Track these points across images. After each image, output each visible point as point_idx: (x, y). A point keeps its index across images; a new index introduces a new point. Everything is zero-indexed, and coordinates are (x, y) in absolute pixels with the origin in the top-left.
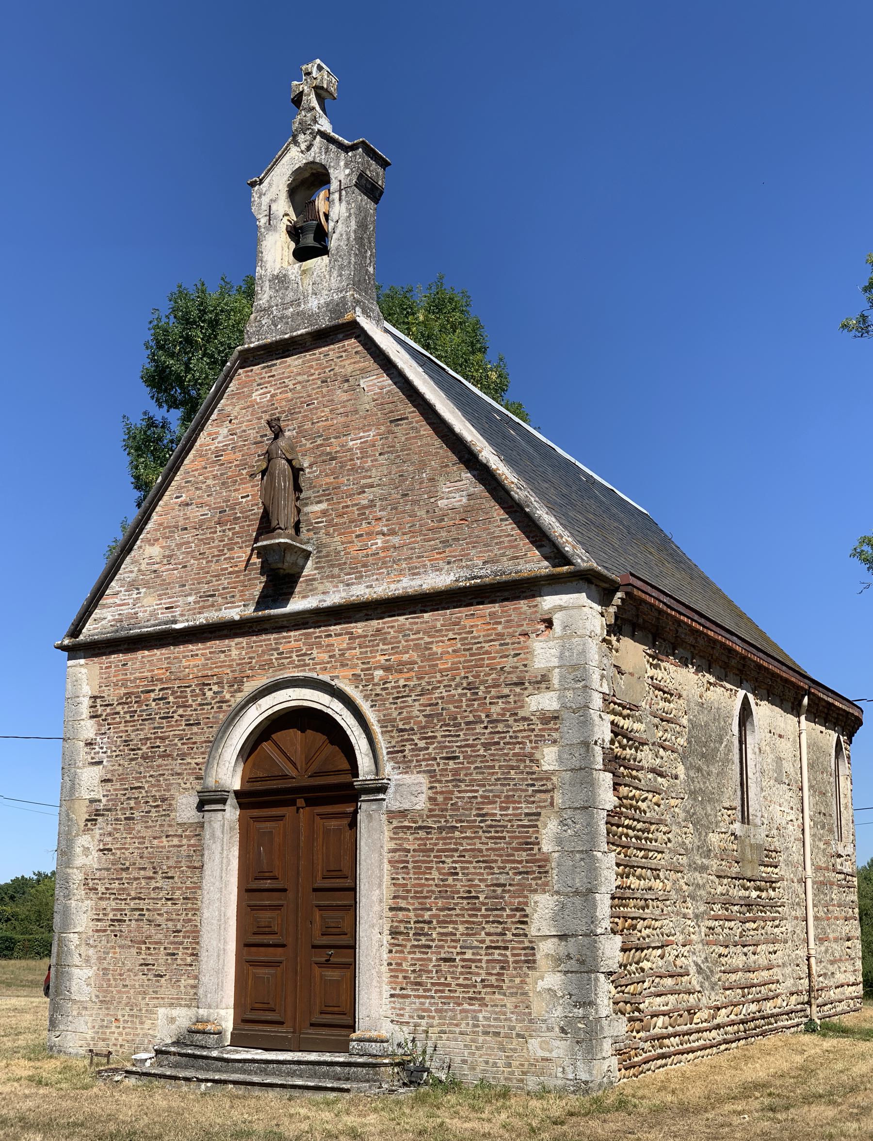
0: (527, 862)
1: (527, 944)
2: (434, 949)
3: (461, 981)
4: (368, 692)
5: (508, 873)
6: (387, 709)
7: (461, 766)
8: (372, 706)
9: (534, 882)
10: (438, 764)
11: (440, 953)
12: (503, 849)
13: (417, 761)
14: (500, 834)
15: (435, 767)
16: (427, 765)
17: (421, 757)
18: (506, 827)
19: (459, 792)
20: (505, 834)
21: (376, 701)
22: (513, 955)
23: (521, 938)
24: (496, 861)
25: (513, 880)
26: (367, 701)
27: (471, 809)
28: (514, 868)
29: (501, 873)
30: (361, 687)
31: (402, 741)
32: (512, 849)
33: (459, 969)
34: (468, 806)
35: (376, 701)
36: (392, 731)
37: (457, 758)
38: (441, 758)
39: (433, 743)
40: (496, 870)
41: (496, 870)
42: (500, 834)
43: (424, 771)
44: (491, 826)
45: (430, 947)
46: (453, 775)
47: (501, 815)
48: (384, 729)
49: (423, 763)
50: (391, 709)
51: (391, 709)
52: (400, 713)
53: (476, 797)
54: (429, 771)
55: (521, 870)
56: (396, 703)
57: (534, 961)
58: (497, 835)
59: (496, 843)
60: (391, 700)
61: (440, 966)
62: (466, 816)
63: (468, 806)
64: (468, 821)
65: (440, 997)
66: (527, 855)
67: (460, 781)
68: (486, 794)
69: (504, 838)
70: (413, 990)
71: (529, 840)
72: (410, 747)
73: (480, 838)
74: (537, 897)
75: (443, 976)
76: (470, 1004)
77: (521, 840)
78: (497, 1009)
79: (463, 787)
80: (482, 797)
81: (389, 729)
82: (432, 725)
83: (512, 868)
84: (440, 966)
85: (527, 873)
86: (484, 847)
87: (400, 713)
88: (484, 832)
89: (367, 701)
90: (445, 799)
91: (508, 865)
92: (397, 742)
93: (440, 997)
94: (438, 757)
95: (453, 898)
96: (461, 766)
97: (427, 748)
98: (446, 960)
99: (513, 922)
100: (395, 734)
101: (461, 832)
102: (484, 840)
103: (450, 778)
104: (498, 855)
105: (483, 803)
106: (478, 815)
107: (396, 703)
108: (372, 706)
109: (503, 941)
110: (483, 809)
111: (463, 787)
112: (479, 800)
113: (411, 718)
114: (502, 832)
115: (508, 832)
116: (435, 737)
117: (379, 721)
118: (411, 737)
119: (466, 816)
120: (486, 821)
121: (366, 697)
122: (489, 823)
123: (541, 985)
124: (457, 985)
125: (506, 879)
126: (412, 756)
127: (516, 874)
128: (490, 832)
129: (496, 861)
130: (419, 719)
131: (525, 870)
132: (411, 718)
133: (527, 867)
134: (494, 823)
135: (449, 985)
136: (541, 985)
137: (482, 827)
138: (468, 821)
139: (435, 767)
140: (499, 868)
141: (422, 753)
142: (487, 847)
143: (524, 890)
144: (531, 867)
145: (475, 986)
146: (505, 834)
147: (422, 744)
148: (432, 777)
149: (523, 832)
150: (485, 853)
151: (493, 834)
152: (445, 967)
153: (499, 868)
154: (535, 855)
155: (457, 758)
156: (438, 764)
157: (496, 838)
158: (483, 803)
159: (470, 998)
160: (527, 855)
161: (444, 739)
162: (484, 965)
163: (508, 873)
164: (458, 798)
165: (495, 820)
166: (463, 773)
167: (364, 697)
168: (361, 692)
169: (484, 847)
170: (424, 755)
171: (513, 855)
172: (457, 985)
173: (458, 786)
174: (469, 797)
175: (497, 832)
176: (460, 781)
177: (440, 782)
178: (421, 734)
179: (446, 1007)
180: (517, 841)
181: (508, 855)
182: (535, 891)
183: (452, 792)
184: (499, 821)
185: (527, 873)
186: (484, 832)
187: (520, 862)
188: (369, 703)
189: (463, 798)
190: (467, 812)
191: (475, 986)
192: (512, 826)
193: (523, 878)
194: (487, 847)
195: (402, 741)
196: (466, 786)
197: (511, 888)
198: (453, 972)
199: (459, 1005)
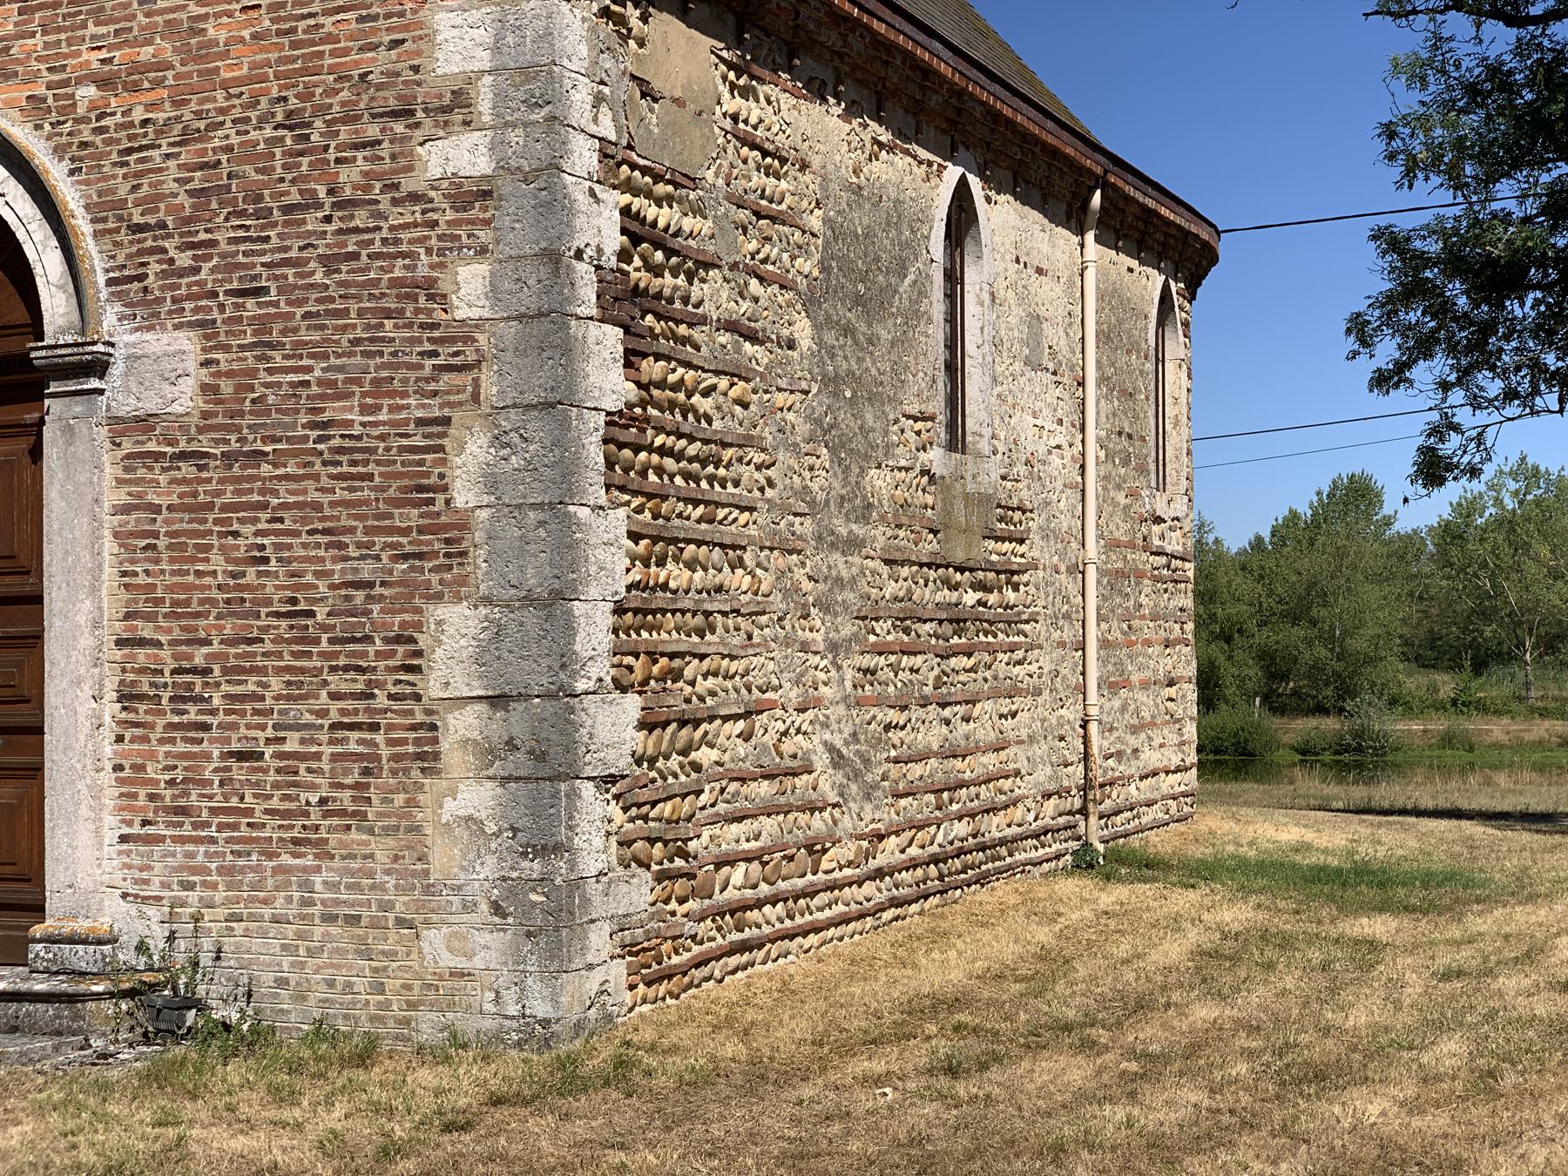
0: (420, 531)
1: (420, 718)
2: (215, 733)
3: (275, 803)
4: (64, 139)
5: (378, 558)
6: (106, 178)
7: (273, 310)
8: (72, 172)
9: (435, 578)
10: (222, 307)
11: (228, 741)
12: (367, 502)
13: (174, 300)
14: (361, 469)
15: (215, 314)
16: (196, 310)
17: (183, 291)
18: (372, 451)
19: (270, 371)
20: (371, 467)
21: (81, 159)
22: (391, 743)
23: (408, 705)
24: (351, 530)
25: (391, 572)
26: (61, 159)
27: (297, 411)
28: (392, 546)
29: (363, 558)
30: (47, 127)
31: (140, 253)
32: (387, 501)
33: (272, 777)
34: (290, 404)
35: (80, 159)
36: (117, 230)
37: (262, 291)
38: (227, 293)
39: (209, 257)
40: (352, 552)
41: (352, 552)
42: (361, 469)
43: (190, 325)
44: (340, 450)
45: (205, 727)
46: (255, 333)
47: (363, 424)
48: (100, 226)
49: (188, 305)
50: (114, 177)
51: (114, 177)
52: (135, 188)
53: (306, 384)
54: (200, 324)
55: (408, 549)
56: (126, 164)
57: (436, 756)
58: (354, 470)
59: (351, 489)
60: (115, 157)
61: (229, 769)
62: (287, 427)
63: (290, 404)
64: (289, 440)
65: (228, 841)
66: (421, 516)
67: (271, 346)
68: (330, 376)
69: (370, 477)
70: (169, 825)
71: (425, 481)
72: (158, 268)
73: (317, 477)
74: (442, 611)
75: (235, 792)
76: (295, 855)
77: (406, 482)
78: (355, 865)
79: (278, 359)
80: (320, 382)
81: (111, 225)
82: (207, 215)
83: (386, 546)
84: (229, 769)
85: (420, 556)
86: (326, 499)
87: (135, 188)
88: (325, 463)
89: (61, 159)
90: (239, 388)
91: (379, 540)
92: (129, 256)
93: (228, 841)
94: (221, 290)
95: (258, 617)
96: (273, 310)
97: (197, 270)
98: (241, 756)
99: (389, 669)
100: (123, 237)
101: (275, 466)
102: (325, 482)
103: (249, 340)
104: (356, 517)
105: (323, 397)
106: (313, 425)
107: (126, 164)
108: (72, 172)
109: (367, 710)
110: (322, 410)
111: (277, 356)
112: (315, 389)
113: (160, 197)
114: (366, 463)
115: (378, 463)
116: (213, 243)
117: (87, 207)
118: (160, 243)
119: (287, 427)
120: (329, 437)
121: (59, 151)
122: (336, 442)
123: (451, 808)
124: (267, 812)
125: (374, 571)
126: (162, 288)
127: (395, 559)
128: (340, 463)
129: (351, 530)
130: (177, 201)
131: (416, 549)
132: (160, 197)
133: (421, 543)
134: (348, 443)
135: (249, 812)
136: (451, 808)
137: (321, 453)
138: (289, 440)
139: (215, 314)
140: (359, 545)
141: (184, 281)
142: (331, 497)
143: (414, 594)
144: (429, 543)
145: (307, 814)
146: (371, 467)
147: (184, 260)
148: (207, 337)
149: (411, 463)
150: (327, 512)
151: (345, 469)
152: (239, 771)
153: (359, 545)
154: (438, 514)
155: (262, 291)
156: (222, 307)
157: (353, 477)
158: (323, 397)
159: (296, 842)
160: (421, 516)
161: (233, 248)
162: (326, 767)
163: (378, 558)
164: (267, 385)
165: (351, 437)
166: (277, 327)
167: (55, 150)
168: (49, 138)
169: (326, 499)
170: (189, 286)
171: (390, 516)
172: (267, 812)
173: (268, 359)
174: (291, 384)
175: (354, 463)
176: (271, 346)
177: (226, 348)
178: (181, 235)
179: (241, 862)
180: (399, 483)
181: (378, 517)
182: (439, 597)
183: (253, 373)
184: (359, 438)
185: (420, 556)
186: (325, 463)
187: (406, 532)
188: (66, 165)
189: (279, 385)
190: (286, 419)
191: (307, 814)
192: (388, 449)
193: (412, 568)
194: (331, 497)
195: (140, 253)
196: (285, 357)
197: (386, 592)
198: (257, 784)
199: (271, 856)
